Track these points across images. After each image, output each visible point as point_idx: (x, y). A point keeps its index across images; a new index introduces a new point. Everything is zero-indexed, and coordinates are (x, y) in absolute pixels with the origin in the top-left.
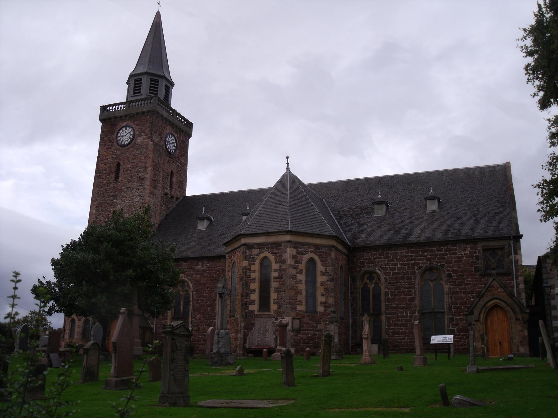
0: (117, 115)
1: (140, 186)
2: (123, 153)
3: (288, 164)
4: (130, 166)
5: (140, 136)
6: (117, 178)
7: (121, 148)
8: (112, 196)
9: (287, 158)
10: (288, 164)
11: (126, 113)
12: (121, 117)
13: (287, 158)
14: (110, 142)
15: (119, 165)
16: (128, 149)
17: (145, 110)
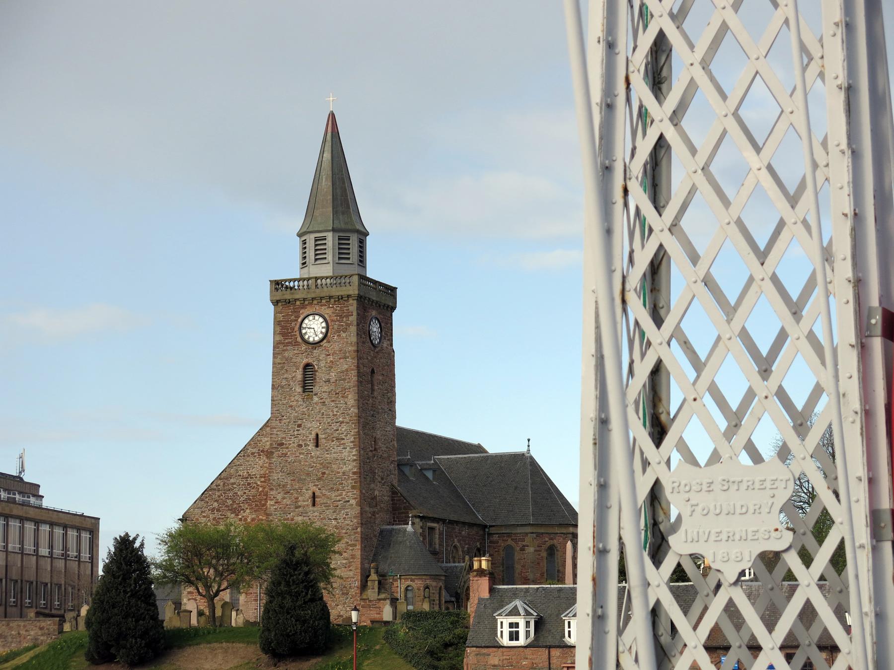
0: (371, 297)
1: (390, 410)
2: (375, 357)
3: (529, 446)
4: (381, 378)
5: (385, 339)
6: (373, 390)
7: (373, 348)
8: (373, 416)
9: (529, 440)
10: (529, 446)
11: (378, 300)
12: (373, 301)
13: (529, 440)
14: (364, 333)
15: (373, 372)
16: (377, 352)
17: (390, 304)
